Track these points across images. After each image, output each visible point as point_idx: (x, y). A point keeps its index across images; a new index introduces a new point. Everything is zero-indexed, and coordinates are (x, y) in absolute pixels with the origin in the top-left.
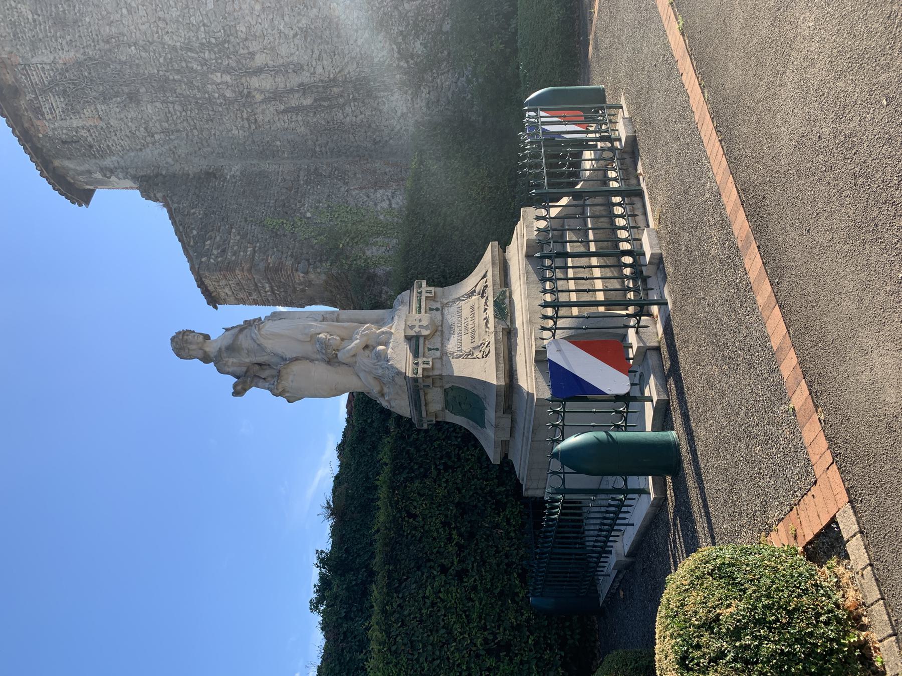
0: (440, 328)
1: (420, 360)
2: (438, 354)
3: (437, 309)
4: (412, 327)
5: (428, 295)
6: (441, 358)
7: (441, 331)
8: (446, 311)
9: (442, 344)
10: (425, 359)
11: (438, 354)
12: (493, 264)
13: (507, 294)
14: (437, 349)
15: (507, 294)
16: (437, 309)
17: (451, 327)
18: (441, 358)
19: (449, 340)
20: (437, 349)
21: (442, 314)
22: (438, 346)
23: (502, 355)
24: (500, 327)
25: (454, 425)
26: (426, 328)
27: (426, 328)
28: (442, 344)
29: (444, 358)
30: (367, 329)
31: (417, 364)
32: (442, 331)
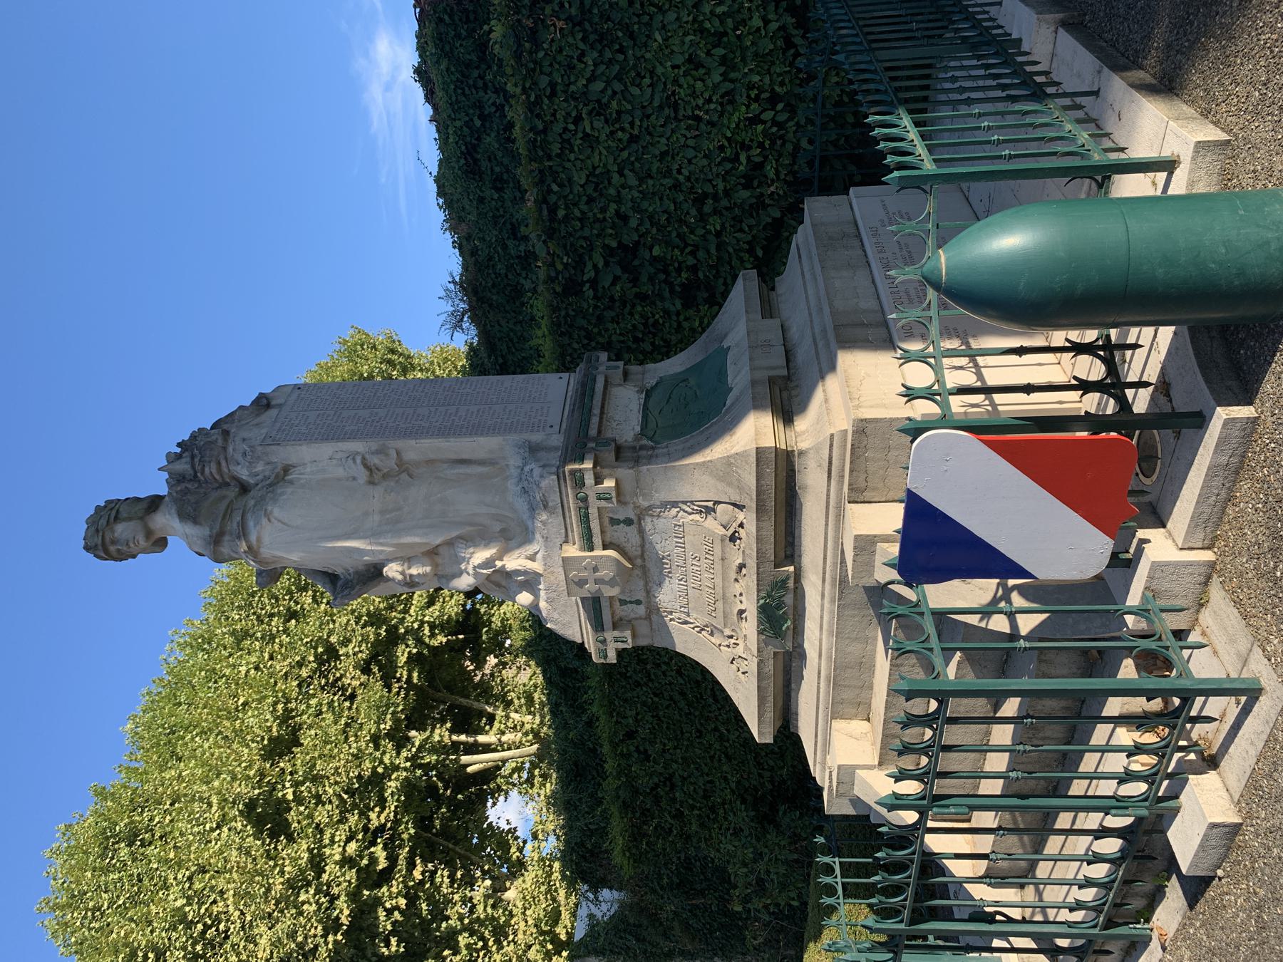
0: (639, 562)
1: (610, 635)
2: (641, 610)
3: (628, 522)
4: (581, 583)
5: (603, 503)
6: (648, 617)
7: (643, 568)
8: (648, 524)
9: (648, 592)
10: (616, 633)
11: (641, 610)
12: (760, 510)
13: (791, 583)
14: (638, 602)
15: (791, 583)
16: (628, 522)
17: (660, 561)
18: (648, 617)
19: (660, 584)
20: (638, 602)
21: (641, 531)
22: (640, 595)
23: (771, 699)
24: (770, 650)
25: (667, 355)
26: (612, 582)
27: (612, 582)
28: (648, 592)
29: (654, 618)
30: (488, 563)
31: (604, 642)
32: (644, 567)
